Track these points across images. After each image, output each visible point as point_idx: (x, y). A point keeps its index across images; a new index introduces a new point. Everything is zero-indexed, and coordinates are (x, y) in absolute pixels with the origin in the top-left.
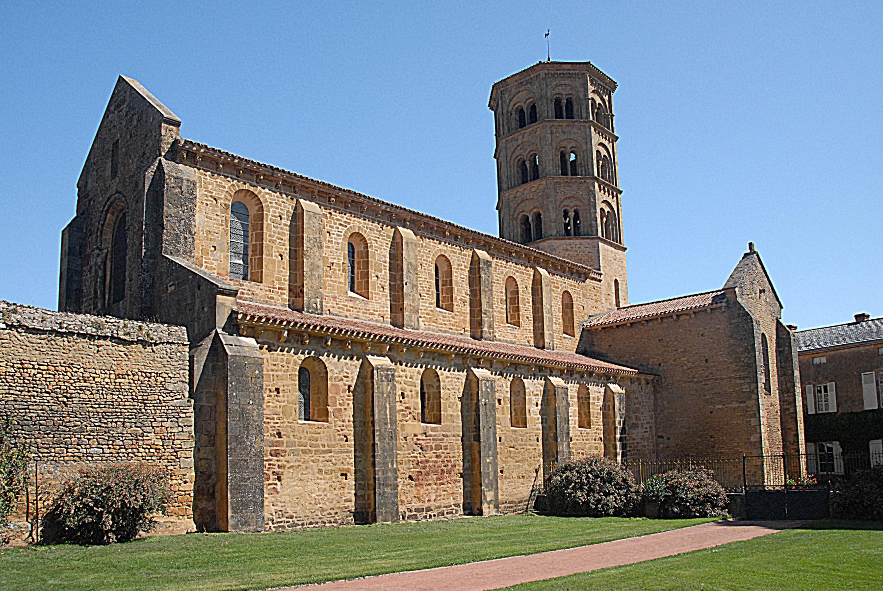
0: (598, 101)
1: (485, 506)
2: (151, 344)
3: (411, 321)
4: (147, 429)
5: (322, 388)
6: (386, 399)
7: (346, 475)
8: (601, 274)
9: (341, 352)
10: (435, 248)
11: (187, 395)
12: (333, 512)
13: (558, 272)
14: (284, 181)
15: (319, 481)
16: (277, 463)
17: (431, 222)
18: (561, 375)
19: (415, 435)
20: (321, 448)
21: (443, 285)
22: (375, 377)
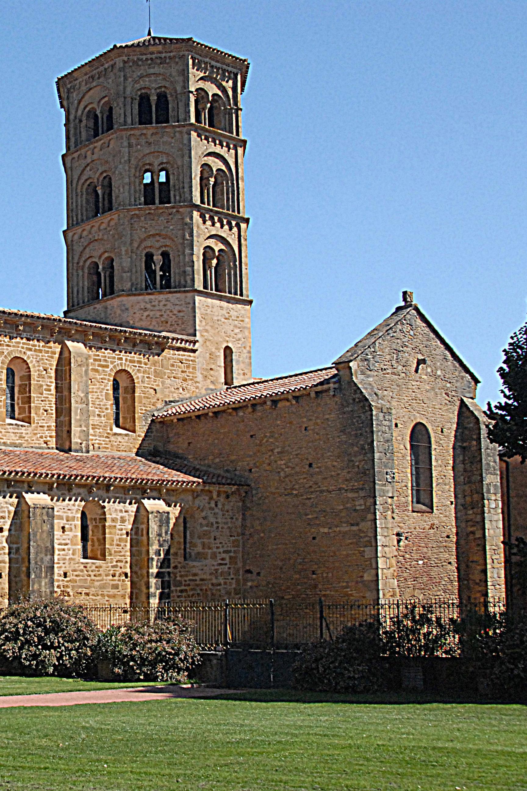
0: (212, 89)
8: (195, 342)
13: (107, 345)
18: (48, 489)
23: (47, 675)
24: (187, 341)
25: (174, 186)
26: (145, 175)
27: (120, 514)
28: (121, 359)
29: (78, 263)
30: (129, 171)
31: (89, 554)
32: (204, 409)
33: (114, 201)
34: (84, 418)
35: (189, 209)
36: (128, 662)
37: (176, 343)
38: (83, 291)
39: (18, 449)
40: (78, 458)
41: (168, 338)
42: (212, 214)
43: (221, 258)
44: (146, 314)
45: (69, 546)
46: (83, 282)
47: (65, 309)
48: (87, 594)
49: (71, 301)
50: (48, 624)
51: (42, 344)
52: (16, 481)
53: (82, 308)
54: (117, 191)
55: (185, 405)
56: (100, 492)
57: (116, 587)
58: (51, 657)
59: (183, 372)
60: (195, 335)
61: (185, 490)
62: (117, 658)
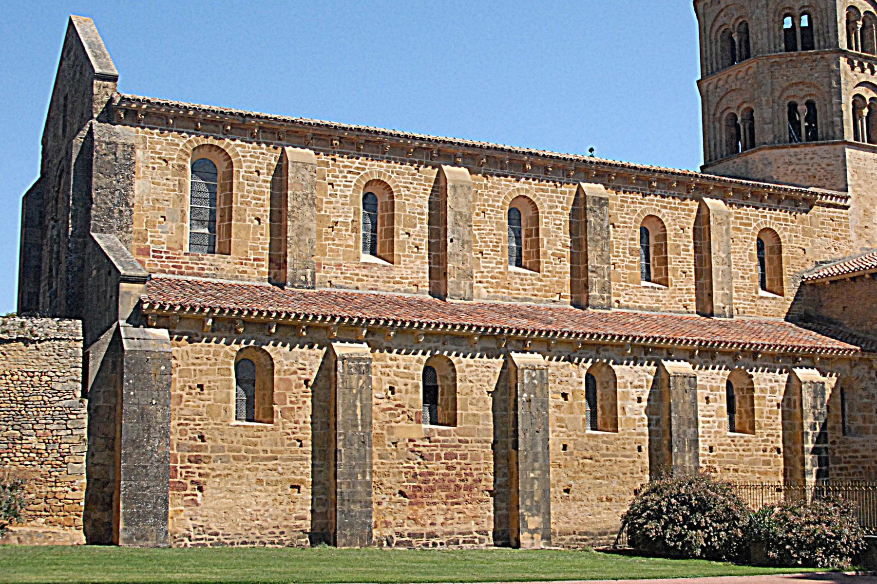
1: (524, 538)
2: (34, 342)
3: (459, 288)
4: (27, 432)
5: (268, 384)
6: (355, 395)
7: (299, 487)
8: (847, 198)
9: (296, 339)
10: (508, 188)
11: (79, 394)
12: (277, 531)
13: (749, 202)
14: (260, 128)
15: (257, 493)
16: (198, 471)
17: (497, 155)
18: (689, 357)
19: (410, 440)
20: (262, 454)
21: (527, 236)
22: (340, 369)
23: (695, 557)
24: (837, 197)
25: (818, 31)
26: (785, 20)
27: (770, 384)
28: (765, 217)
29: (714, 115)
30: (767, 16)
31: (737, 427)
32: (859, 270)
33: (751, 48)
34: (726, 280)
35: (835, 55)
36: (784, 545)
37: (826, 199)
38: (721, 144)
39: (655, 313)
40: (721, 323)
41: (817, 194)
42: (860, 59)
43: (872, 106)
44: (791, 168)
45: (714, 418)
46: (721, 135)
47: (702, 163)
48: (736, 470)
49: (708, 155)
50: (694, 502)
51: (678, 201)
52: (654, 348)
53: (720, 162)
54: (754, 37)
55: (838, 266)
56: (747, 360)
57: (768, 463)
58: (698, 538)
59: (834, 230)
60: (847, 191)
61: (841, 359)
62: (770, 541)
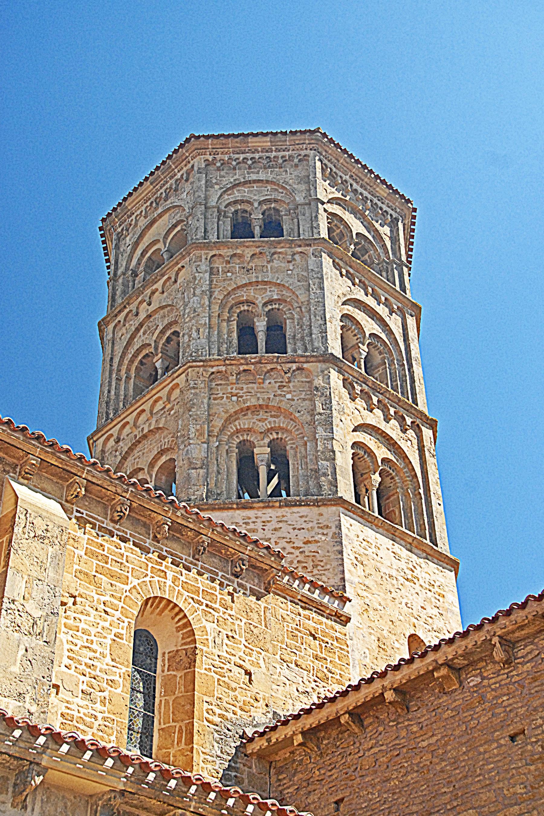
8: (344, 600)
